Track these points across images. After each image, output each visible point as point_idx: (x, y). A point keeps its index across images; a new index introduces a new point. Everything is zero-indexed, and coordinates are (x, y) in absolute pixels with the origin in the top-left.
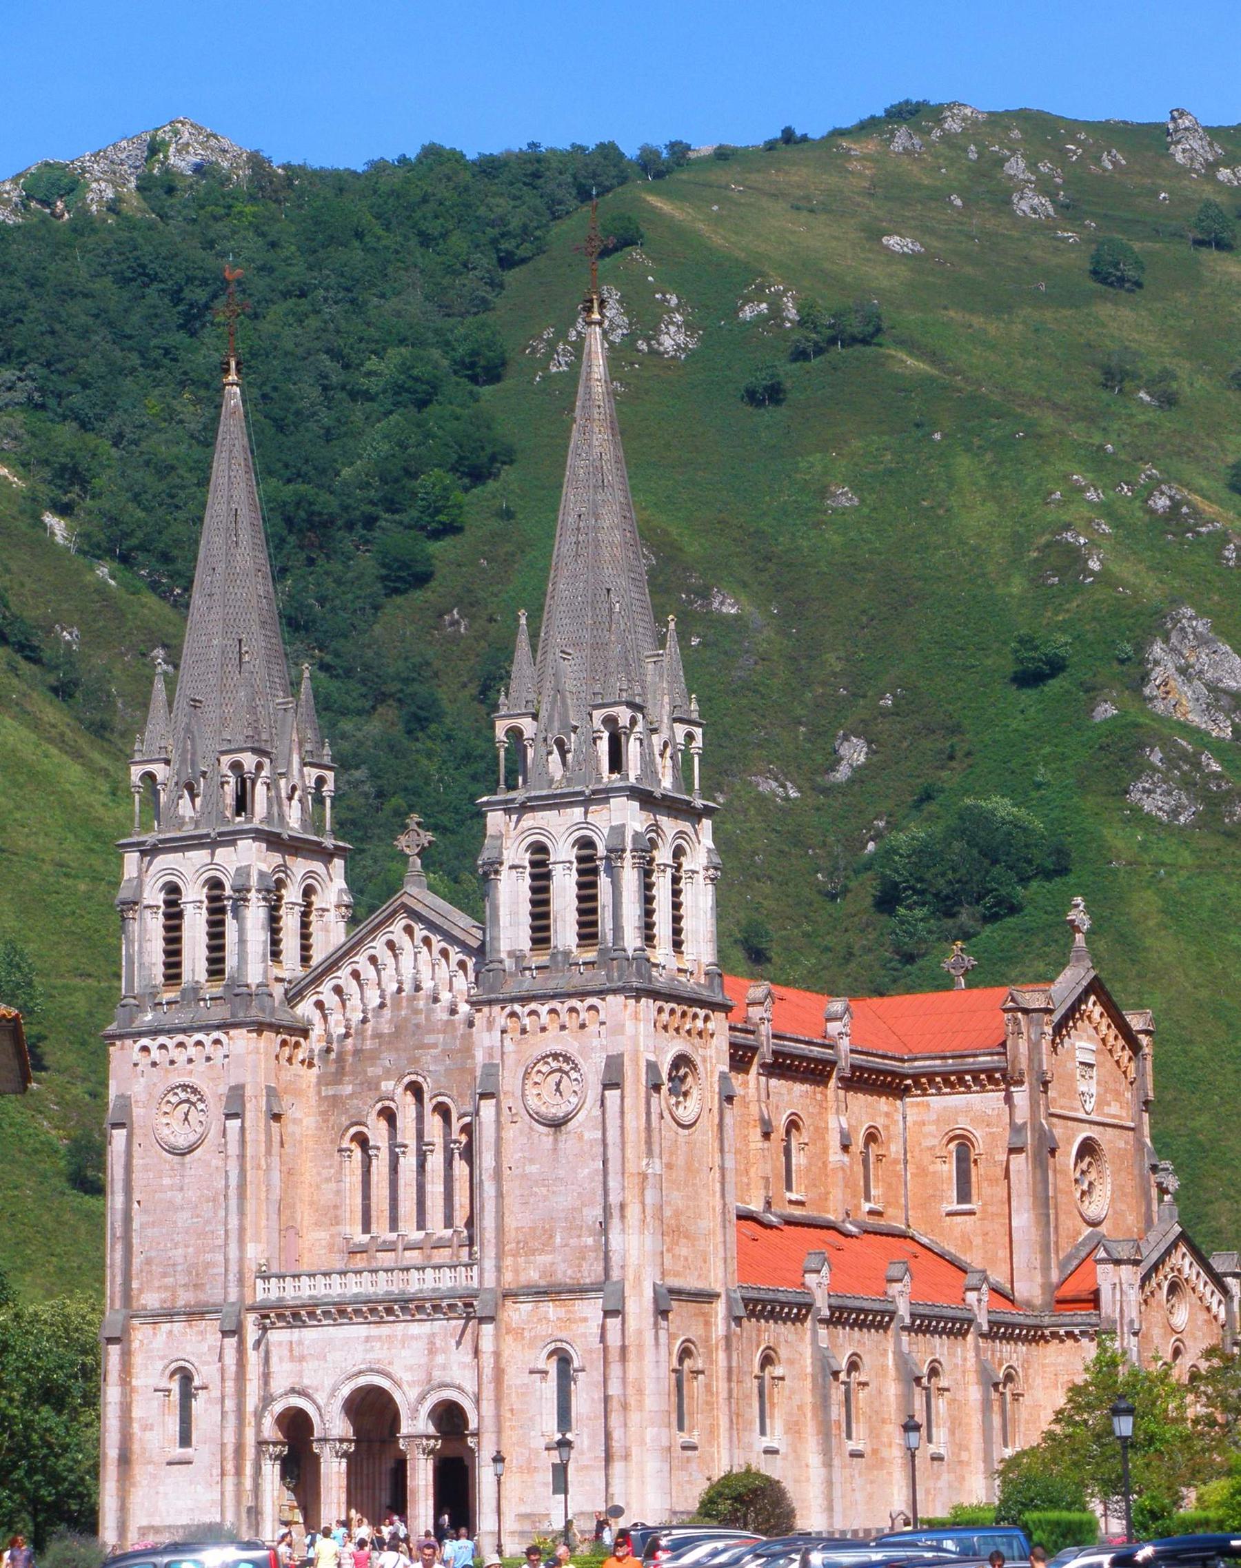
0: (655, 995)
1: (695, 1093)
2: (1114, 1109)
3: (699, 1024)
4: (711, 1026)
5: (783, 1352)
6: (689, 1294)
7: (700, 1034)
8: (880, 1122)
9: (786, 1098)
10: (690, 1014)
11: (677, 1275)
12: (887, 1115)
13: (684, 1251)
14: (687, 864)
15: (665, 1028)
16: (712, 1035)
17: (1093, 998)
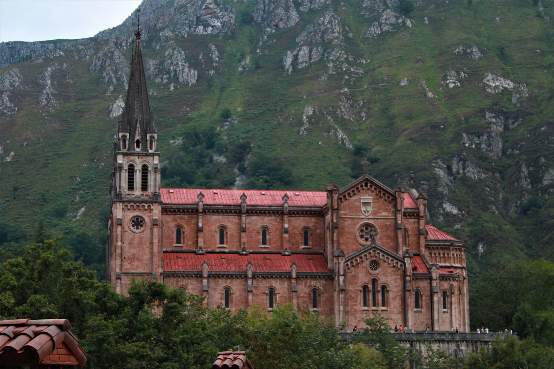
0: (123, 202)
1: (144, 225)
2: (384, 214)
3: (146, 208)
4: (152, 208)
5: (190, 287)
6: (137, 273)
7: (146, 210)
8: (311, 225)
9: (260, 221)
10: (141, 205)
11: (133, 269)
12: (315, 222)
13: (137, 264)
14: (149, 169)
15: (129, 209)
16: (152, 210)
17: (369, 185)
